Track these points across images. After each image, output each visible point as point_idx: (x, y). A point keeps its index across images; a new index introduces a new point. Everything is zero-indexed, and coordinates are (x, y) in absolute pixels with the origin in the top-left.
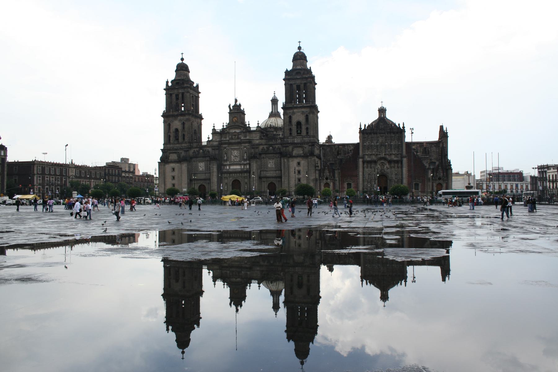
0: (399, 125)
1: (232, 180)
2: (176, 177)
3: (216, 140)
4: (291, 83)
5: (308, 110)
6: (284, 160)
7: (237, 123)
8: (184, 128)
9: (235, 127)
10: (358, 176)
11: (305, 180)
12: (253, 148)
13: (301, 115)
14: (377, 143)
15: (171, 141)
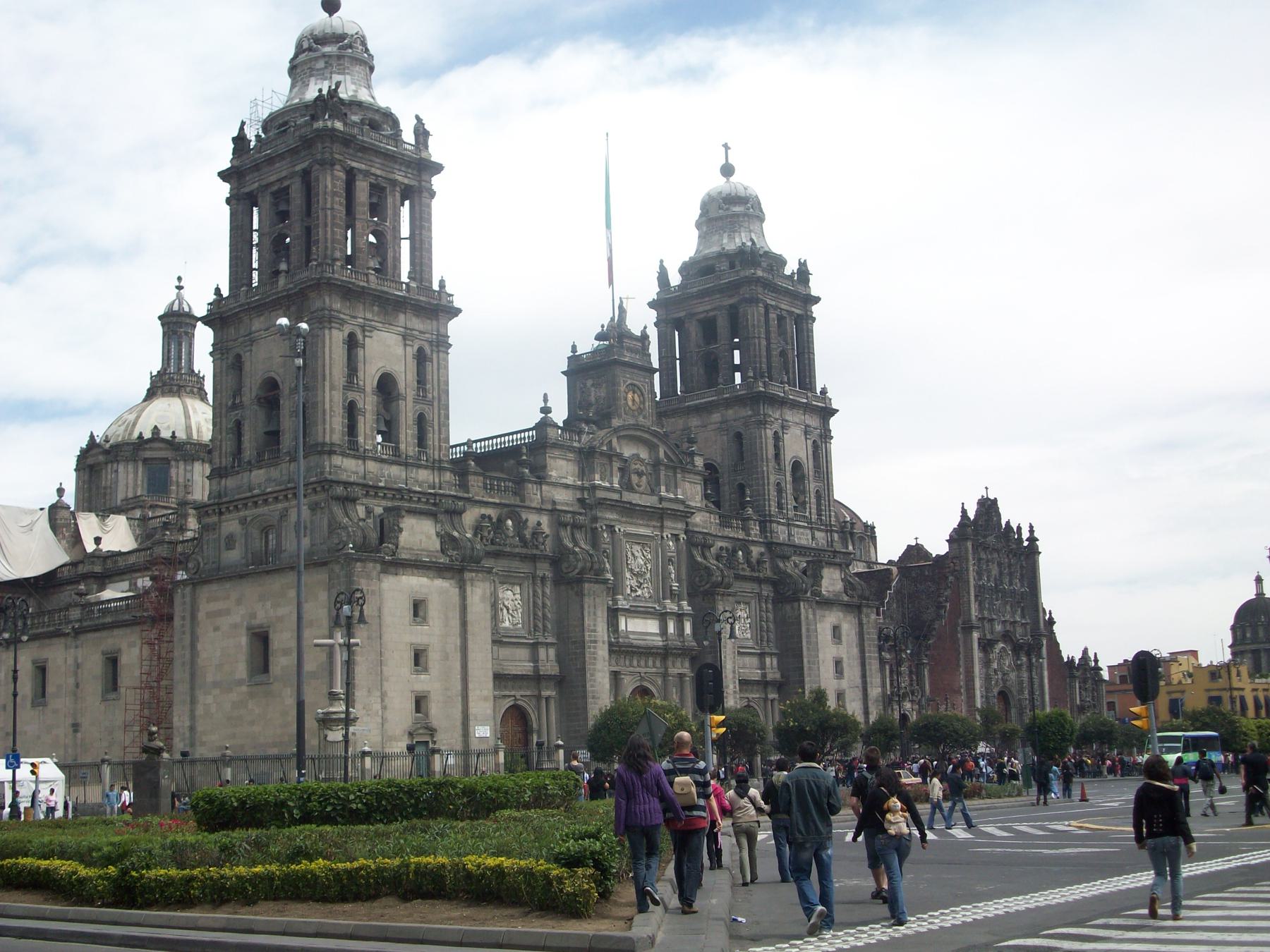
0: (1019, 528)
1: (630, 690)
2: (433, 657)
3: (564, 481)
4: (769, 302)
5: (813, 421)
6: (807, 612)
7: (641, 418)
8: (421, 381)
9: (639, 433)
10: (962, 690)
11: (854, 700)
12: (696, 545)
13: (803, 438)
14: (989, 580)
15: (361, 439)
